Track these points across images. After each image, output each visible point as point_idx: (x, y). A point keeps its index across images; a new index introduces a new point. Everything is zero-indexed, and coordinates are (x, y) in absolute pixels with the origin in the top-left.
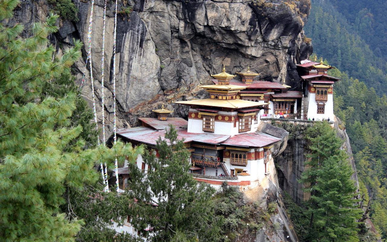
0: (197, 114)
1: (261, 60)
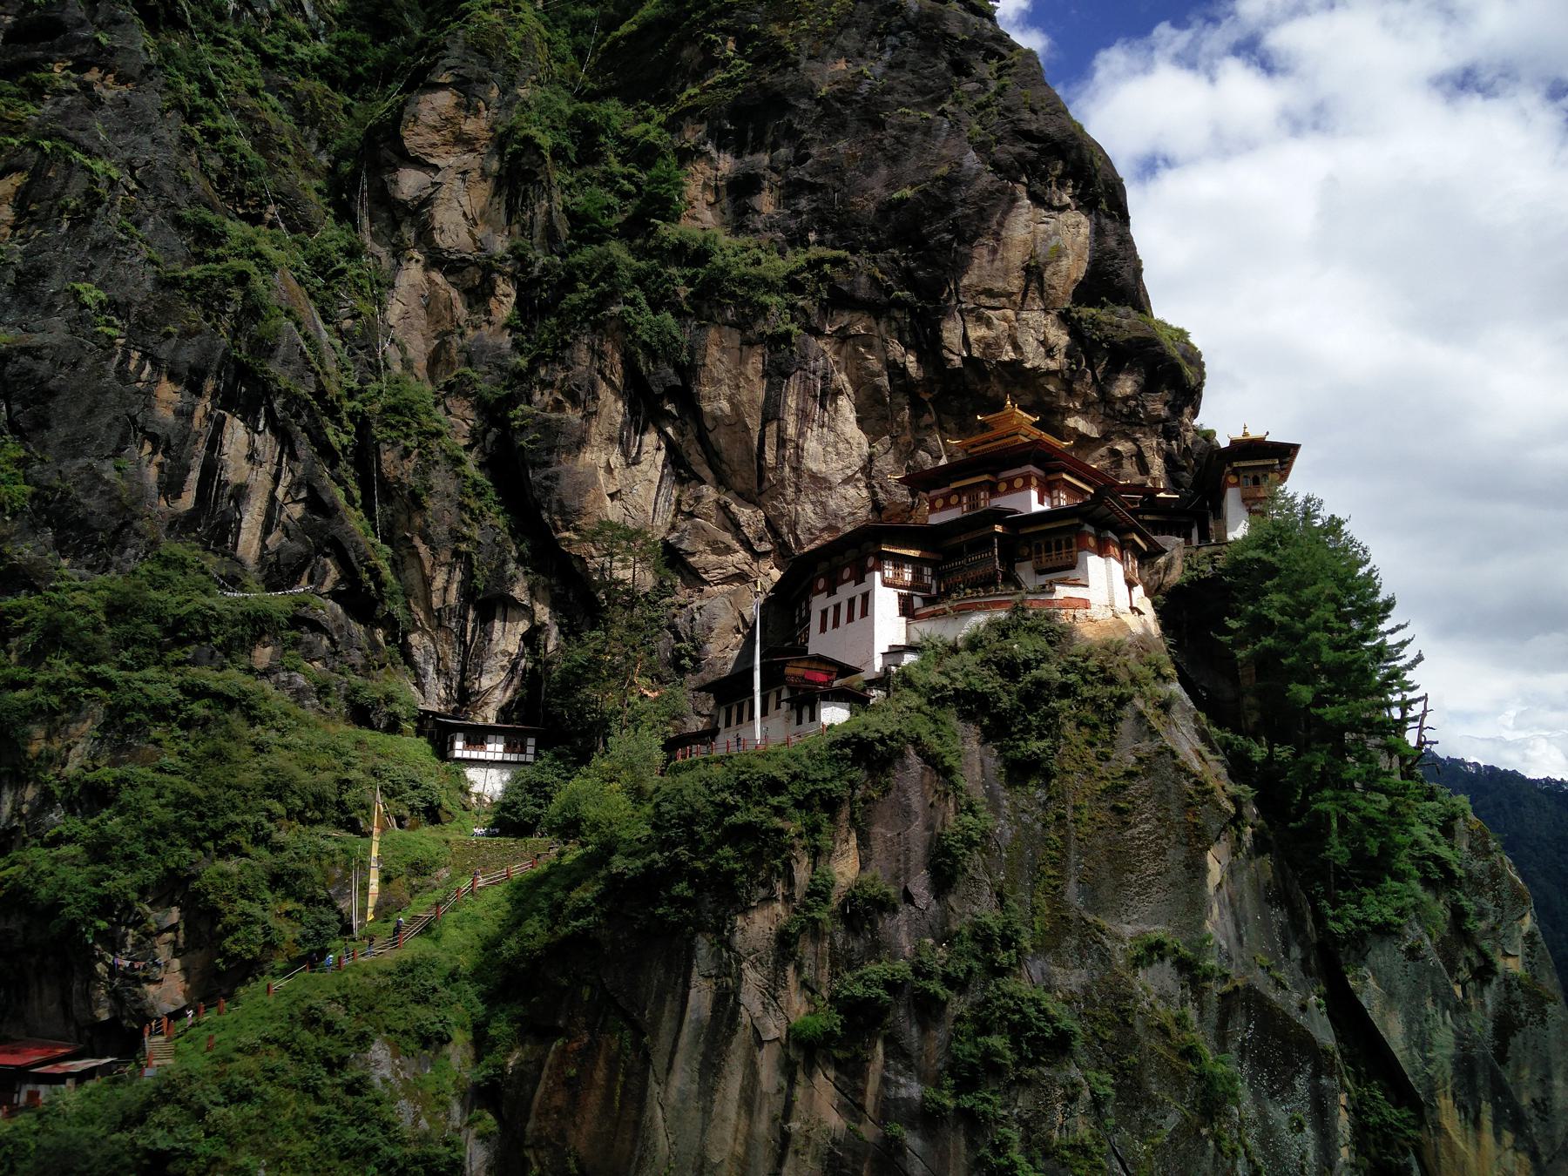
0: (946, 498)
1: (1103, 450)
